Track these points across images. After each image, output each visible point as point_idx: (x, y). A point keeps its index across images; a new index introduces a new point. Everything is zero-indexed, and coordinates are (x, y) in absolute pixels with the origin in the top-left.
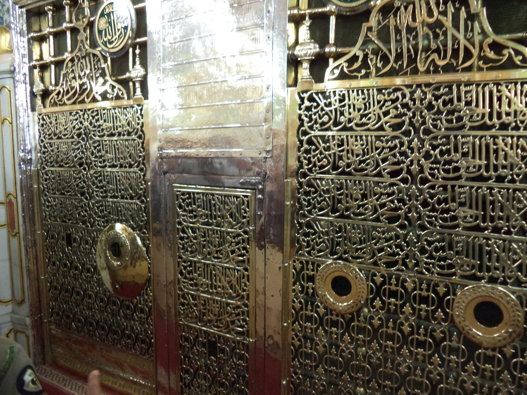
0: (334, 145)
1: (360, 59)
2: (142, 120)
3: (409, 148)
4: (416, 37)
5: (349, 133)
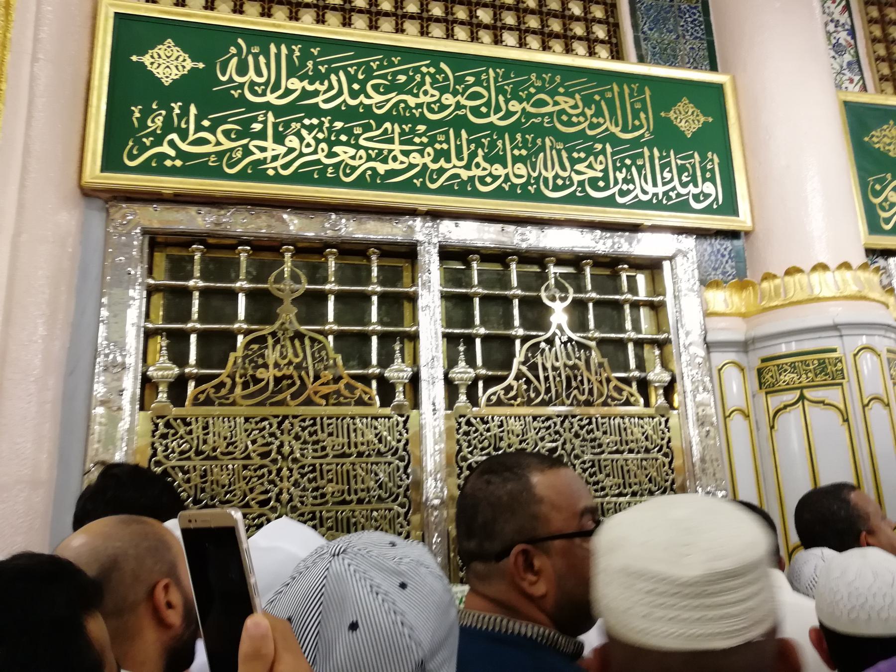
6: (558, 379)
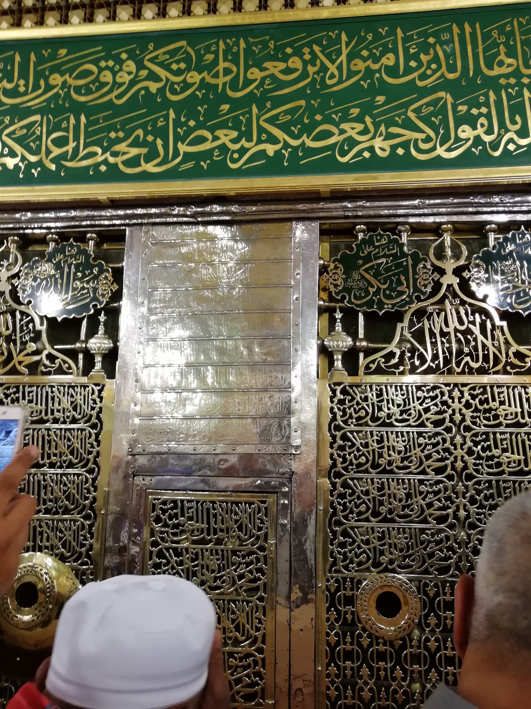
0: (373, 441)
1: (397, 356)
2: (99, 405)
3: (452, 444)
4: (449, 341)
5: (390, 429)
6: (447, 345)
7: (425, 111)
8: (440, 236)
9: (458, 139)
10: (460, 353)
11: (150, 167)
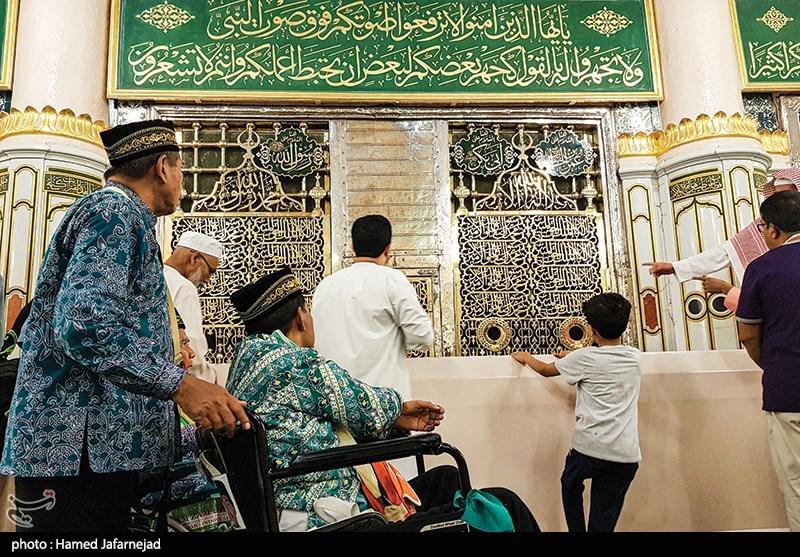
7: (511, 57)
8: (517, 131)
9: (528, 75)
10: (529, 198)
11: (346, 83)
